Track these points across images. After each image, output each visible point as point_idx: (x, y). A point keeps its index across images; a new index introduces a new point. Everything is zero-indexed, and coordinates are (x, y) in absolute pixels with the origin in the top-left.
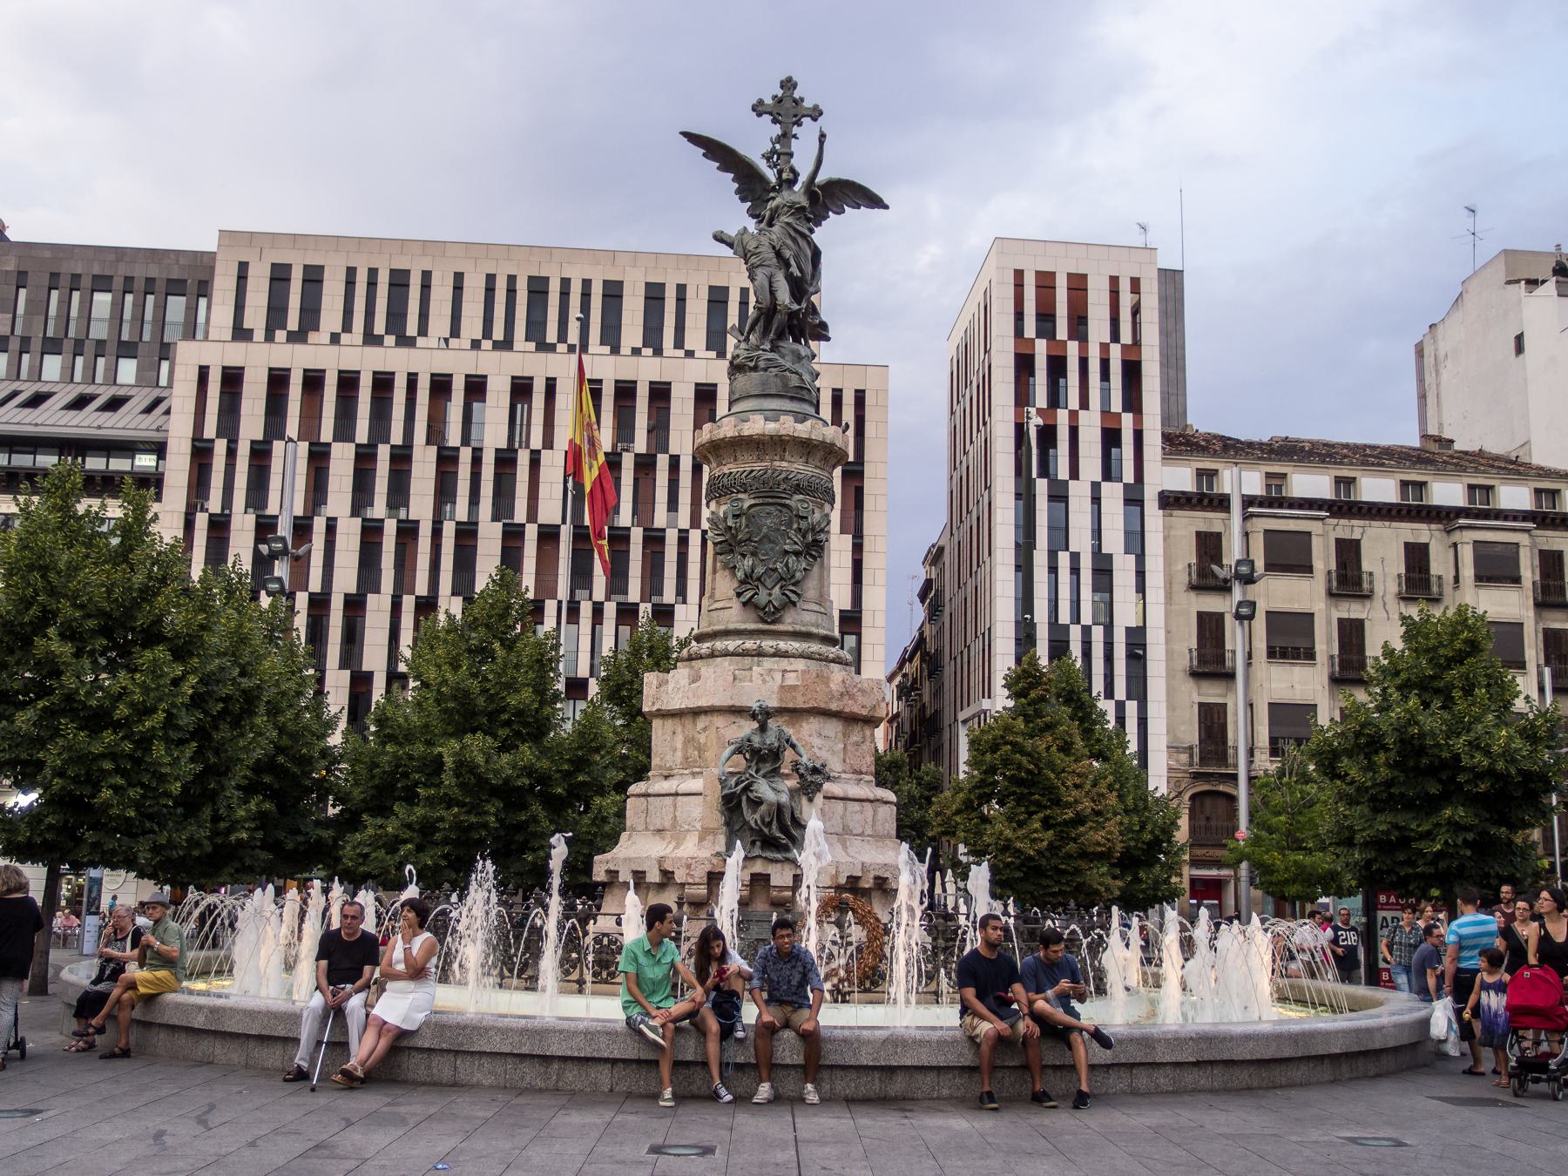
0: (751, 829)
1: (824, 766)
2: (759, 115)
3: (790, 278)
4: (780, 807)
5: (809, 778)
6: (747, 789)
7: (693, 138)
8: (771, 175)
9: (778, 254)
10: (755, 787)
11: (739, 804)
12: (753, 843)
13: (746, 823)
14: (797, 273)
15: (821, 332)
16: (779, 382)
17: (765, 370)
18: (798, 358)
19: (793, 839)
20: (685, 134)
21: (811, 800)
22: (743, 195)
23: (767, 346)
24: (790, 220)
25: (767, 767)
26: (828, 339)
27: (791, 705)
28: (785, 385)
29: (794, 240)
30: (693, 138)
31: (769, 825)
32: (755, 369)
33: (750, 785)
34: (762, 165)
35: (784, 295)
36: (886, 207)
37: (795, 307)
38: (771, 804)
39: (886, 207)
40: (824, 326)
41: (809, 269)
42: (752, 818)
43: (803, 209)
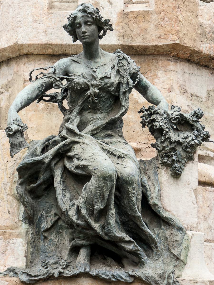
0: (71, 225)
1: (198, 116)
4: (121, 185)
5: (174, 136)
6: (63, 154)
10: (76, 150)
11: (49, 185)
12: (75, 251)
13: (62, 215)
19: (147, 243)
21: (176, 175)
25: (100, 119)
27: (138, 42)
31: (103, 214)
33: (68, 147)
38: (106, 178)
42: (69, 201)
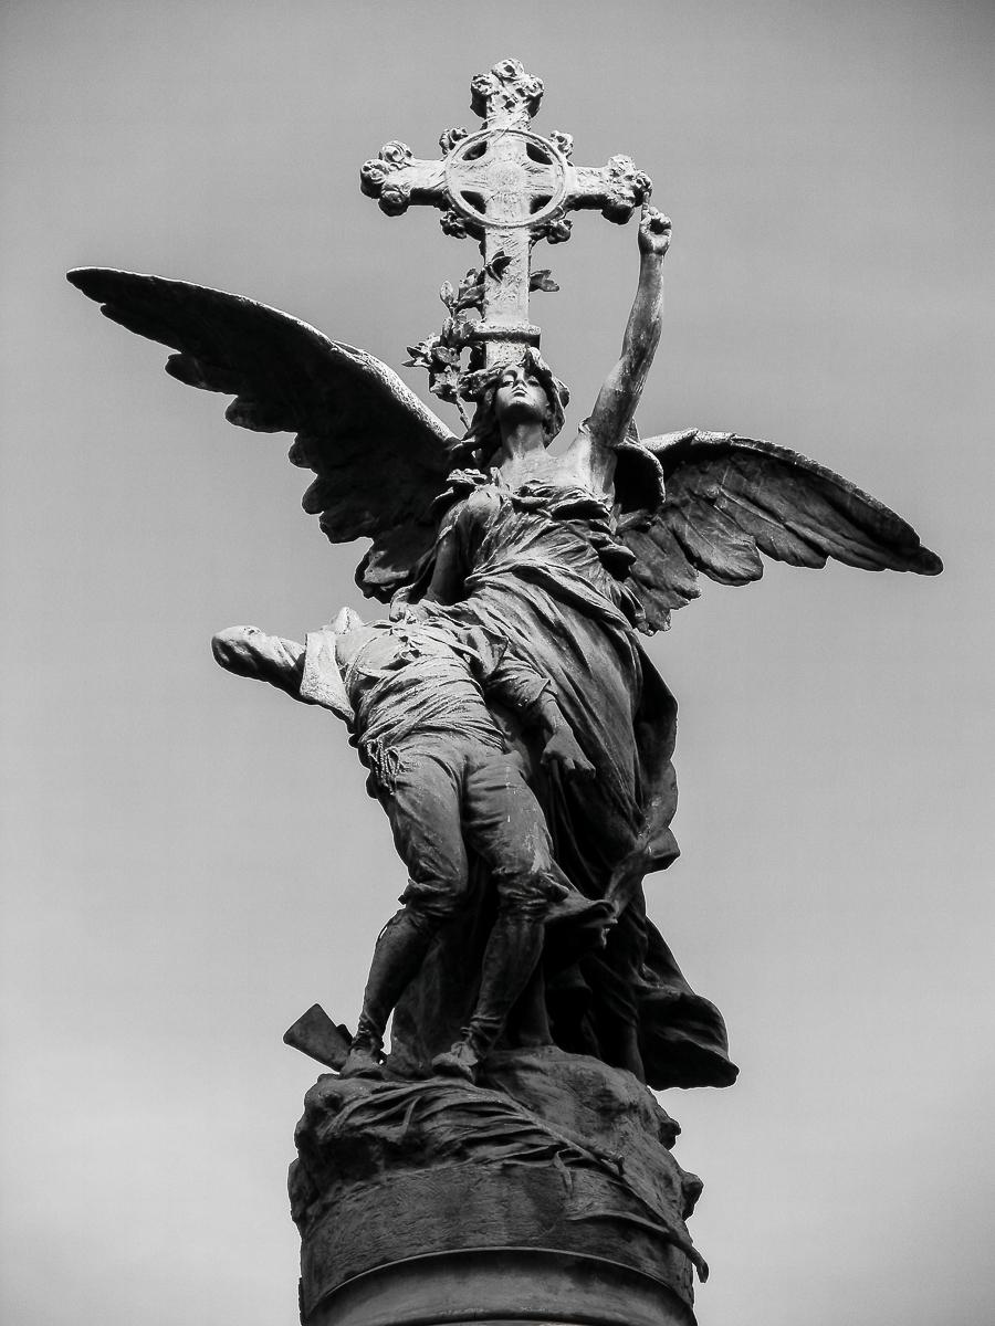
2: (393, 208)
3: (545, 776)
7: (129, 300)
8: (450, 423)
9: (495, 692)
14: (575, 756)
15: (689, 1047)
16: (525, 1206)
17: (460, 1152)
18: (608, 1110)
20: (91, 282)
22: (337, 509)
23: (463, 1056)
24: (538, 557)
26: (723, 1074)
28: (551, 1211)
29: (557, 632)
30: (129, 300)
32: (413, 1152)
34: (409, 388)
35: (530, 842)
36: (928, 564)
37: (577, 901)
39: (928, 564)
40: (704, 1018)
41: (625, 756)
43: (586, 512)
